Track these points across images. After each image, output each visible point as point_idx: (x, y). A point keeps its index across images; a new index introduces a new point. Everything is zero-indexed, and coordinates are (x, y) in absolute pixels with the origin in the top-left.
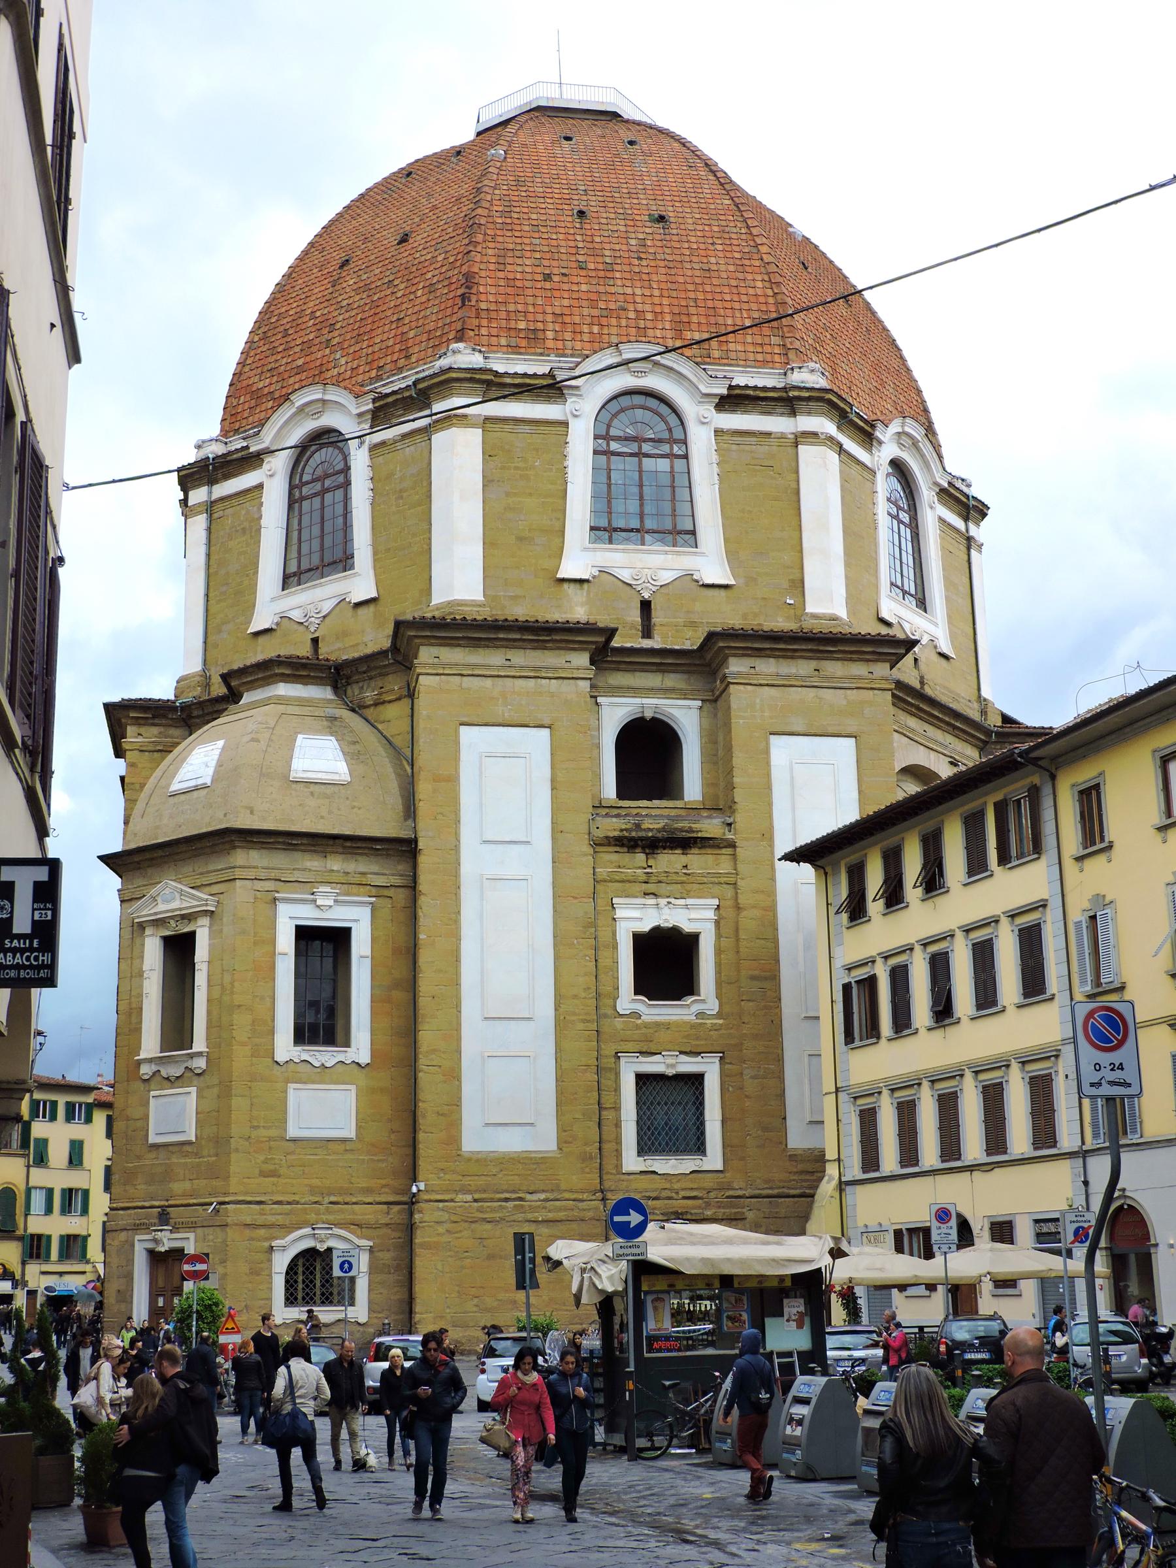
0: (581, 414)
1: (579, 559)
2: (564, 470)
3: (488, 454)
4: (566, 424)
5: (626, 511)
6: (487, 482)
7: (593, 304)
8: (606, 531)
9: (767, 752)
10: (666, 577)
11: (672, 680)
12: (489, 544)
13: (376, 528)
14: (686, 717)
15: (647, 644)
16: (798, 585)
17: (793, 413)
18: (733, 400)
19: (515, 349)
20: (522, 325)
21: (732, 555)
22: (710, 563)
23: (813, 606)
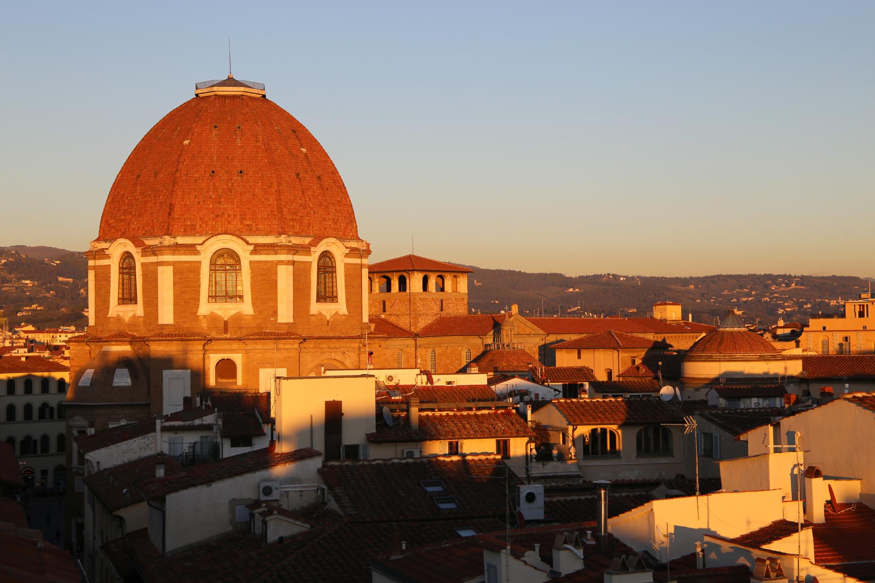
0: (204, 258)
1: (205, 308)
2: (199, 278)
3: (175, 273)
4: (200, 262)
5: (221, 291)
6: (175, 284)
7: (213, 213)
8: (213, 297)
9: (258, 374)
10: (233, 312)
11: (235, 345)
12: (176, 304)
13: (144, 292)
14: (238, 358)
15: (225, 336)
16: (275, 313)
17: (276, 254)
18: (258, 249)
19: (185, 234)
20: (189, 223)
21: (254, 304)
22: (246, 308)
23: (281, 320)
